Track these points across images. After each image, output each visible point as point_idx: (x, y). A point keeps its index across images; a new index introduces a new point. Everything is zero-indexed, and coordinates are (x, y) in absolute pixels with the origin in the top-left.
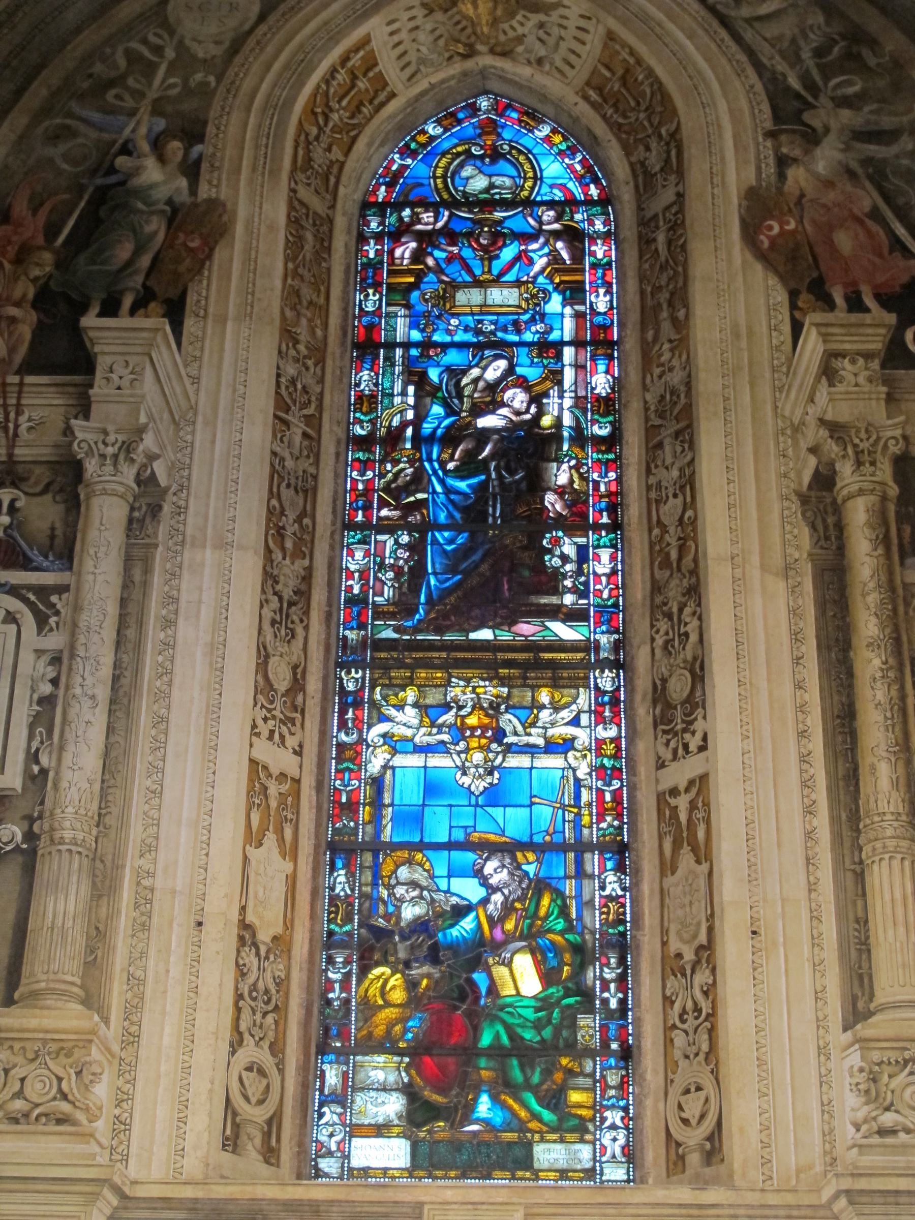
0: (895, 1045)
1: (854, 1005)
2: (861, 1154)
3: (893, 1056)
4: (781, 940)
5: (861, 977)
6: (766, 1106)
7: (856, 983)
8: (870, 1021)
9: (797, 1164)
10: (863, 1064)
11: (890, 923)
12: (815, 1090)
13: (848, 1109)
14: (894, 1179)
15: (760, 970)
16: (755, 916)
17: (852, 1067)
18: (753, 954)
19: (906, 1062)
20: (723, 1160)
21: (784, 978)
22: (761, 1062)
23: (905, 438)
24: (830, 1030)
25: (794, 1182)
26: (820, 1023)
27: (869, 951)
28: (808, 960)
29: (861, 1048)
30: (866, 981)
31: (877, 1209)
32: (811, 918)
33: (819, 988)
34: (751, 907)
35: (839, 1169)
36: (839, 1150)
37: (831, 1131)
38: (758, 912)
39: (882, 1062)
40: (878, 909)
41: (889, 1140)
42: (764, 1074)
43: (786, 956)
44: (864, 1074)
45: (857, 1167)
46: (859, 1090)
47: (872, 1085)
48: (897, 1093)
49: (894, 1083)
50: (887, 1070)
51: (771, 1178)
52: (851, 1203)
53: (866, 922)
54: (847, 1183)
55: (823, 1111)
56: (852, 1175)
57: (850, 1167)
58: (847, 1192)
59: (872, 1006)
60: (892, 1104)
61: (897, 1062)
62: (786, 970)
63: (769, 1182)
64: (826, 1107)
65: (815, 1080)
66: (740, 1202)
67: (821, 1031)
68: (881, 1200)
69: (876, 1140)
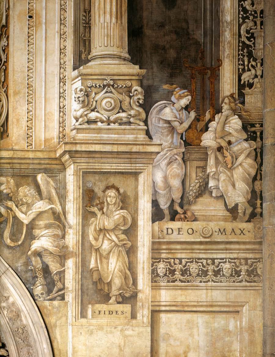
0: (99, 77)
1: (80, 56)
2: (77, 133)
3: (98, 83)
4: (44, 21)
5: (85, 41)
6: (30, 109)
7: (82, 44)
8: (87, 65)
9: (45, 138)
10: (83, 87)
11: (102, 12)
12: (57, 100)
13: (73, 110)
14: (93, 146)
15: (32, 37)
16: (31, 8)
17: (77, 89)
18: (29, 28)
19: (104, 86)
20: (8, 136)
21: (44, 41)
22: (29, 86)
24: (67, 70)
25: (43, 147)
26: (62, 66)
27: (90, 27)
28: (58, 32)
29: (82, 79)
30: (87, 43)
31: (83, 160)
32: (61, 9)
33: (62, 47)
34: (29, 3)
35: (66, 140)
36: (67, 130)
37: (64, 121)
38: (32, 6)
39: (92, 86)
40: (97, 4)
41: (93, 126)
42: (31, 92)
43: (46, 30)
44: (82, 92)
45: (74, 139)
46: (79, 101)
47: (86, 98)
48: (98, 102)
49: (98, 97)
50: (94, 90)
51: (32, 145)
52: (71, 157)
53: (90, 11)
54: (68, 148)
55: (60, 111)
56: (71, 143)
57: (72, 139)
58: (70, 152)
59: (89, 57)
60: (95, 108)
61: (100, 86)
62: (46, 38)
63: (31, 147)
64: (62, 109)
65: (57, 96)
66: (15, 156)
67: (62, 70)
68: (86, 156)
69: (86, 126)
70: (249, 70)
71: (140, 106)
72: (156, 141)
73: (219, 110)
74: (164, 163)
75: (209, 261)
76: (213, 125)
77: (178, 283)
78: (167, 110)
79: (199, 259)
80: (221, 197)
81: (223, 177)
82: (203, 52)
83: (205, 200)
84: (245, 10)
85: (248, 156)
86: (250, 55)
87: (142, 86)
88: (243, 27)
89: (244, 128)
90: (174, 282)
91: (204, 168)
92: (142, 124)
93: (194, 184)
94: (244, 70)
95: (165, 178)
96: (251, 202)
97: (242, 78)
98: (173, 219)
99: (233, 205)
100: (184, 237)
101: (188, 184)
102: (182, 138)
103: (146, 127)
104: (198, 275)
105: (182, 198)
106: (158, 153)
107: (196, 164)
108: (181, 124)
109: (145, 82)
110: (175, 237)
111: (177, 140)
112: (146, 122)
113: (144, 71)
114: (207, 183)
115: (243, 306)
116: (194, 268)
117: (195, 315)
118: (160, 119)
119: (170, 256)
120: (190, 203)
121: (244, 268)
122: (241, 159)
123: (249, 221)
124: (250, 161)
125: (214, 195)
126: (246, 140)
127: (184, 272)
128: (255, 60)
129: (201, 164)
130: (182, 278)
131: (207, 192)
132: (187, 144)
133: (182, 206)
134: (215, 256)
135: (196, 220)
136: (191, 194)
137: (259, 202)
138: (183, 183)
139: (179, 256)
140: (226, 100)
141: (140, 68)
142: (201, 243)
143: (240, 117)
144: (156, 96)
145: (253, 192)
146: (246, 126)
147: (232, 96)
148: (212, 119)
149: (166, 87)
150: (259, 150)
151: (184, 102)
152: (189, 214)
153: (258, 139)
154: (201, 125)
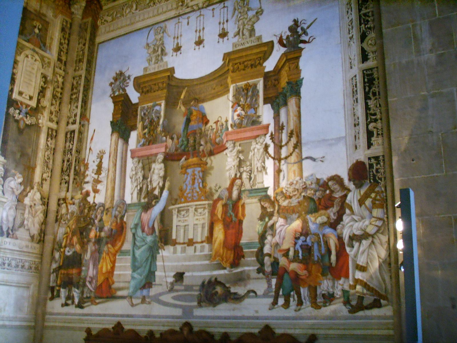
23: (27, 3)
70: (46, 173)
71: (2, 177)
72: (6, 196)
73: (32, 188)
74: (7, 208)
75: (20, 261)
76: (30, 194)
77: (6, 270)
78: (12, 183)
79: (16, 259)
80: (28, 230)
81: (30, 220)
82: (30, 160)
83: (22, 230)
84: (48, 146)
85: (41, 212)
86: (47, 167)
87: (4, 168)
88: (46, 153)
89: (41, 199)
90: (4, 269)
91: (23, 214)
92: (1, 186)
93: (18, 222)
94: (44, 172)
95: (7, 216)
96: (40, 235)
97: (43, 176)
98: (8, 237)
99: (33, 234)
100: (11, 247)
101: (16, 220)
102: (17, 198)
103: (2, 188)
104: (15, 267)
105: (13, 227)
106: (6, 203)
107: (21, 211)
108: (17, 190)
109: (5, 166)
110: (7, 246)
111: (14, 198)
112: (3, 186)
113: (5, 161)
114: (24, 222)
115: (31, 284)
116: (13, 263)
117: (11, 287)
118: (9, 186)
119: (5, 256)
120: (15, 230)
121: (34, 266)
122: (39, 212)
123: (38, 243)
124: (42, 215)
125: (26, 228)
126: (42, 205)
127: (9, 265)
128: (49, 169)
129: (23, 212)
130: (8, 267)
131: (23, 226)
132: (18, 201)
133: (12, 231)
134: (23, 258)
135: (17, 238)
136: (17, 226)
137: (43, 235)
138: (14, 219)
139: (8, 256)
140: (36, 184)
141: (5, 159)
142: (17, 251)
143: (40, 193)
144: (8, 174)
145: (41, 230)
146: (42, 198)
147: (38, 183)
148: (29, 192)
149: (13, 171)
150: (46, 211)
151: (20, 180)
152: (14, 236)
153: (46, 205)
154: (25, 193)
